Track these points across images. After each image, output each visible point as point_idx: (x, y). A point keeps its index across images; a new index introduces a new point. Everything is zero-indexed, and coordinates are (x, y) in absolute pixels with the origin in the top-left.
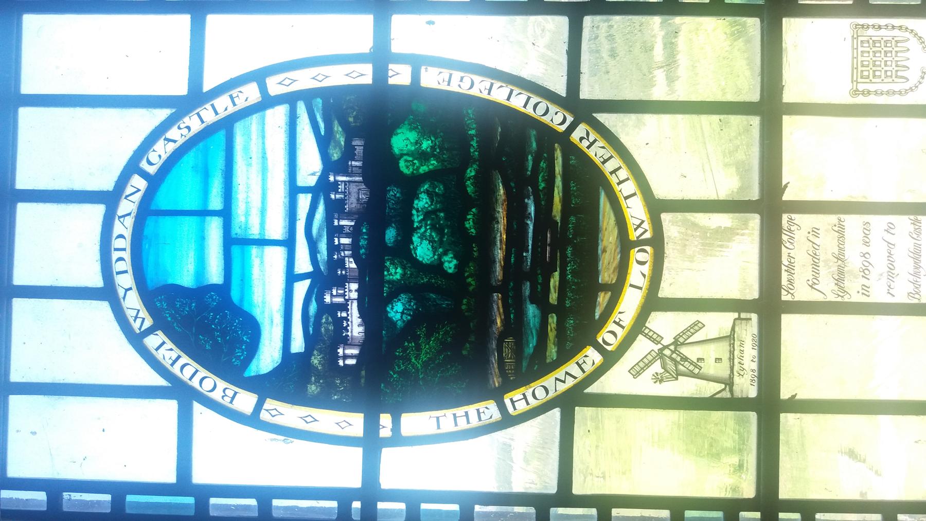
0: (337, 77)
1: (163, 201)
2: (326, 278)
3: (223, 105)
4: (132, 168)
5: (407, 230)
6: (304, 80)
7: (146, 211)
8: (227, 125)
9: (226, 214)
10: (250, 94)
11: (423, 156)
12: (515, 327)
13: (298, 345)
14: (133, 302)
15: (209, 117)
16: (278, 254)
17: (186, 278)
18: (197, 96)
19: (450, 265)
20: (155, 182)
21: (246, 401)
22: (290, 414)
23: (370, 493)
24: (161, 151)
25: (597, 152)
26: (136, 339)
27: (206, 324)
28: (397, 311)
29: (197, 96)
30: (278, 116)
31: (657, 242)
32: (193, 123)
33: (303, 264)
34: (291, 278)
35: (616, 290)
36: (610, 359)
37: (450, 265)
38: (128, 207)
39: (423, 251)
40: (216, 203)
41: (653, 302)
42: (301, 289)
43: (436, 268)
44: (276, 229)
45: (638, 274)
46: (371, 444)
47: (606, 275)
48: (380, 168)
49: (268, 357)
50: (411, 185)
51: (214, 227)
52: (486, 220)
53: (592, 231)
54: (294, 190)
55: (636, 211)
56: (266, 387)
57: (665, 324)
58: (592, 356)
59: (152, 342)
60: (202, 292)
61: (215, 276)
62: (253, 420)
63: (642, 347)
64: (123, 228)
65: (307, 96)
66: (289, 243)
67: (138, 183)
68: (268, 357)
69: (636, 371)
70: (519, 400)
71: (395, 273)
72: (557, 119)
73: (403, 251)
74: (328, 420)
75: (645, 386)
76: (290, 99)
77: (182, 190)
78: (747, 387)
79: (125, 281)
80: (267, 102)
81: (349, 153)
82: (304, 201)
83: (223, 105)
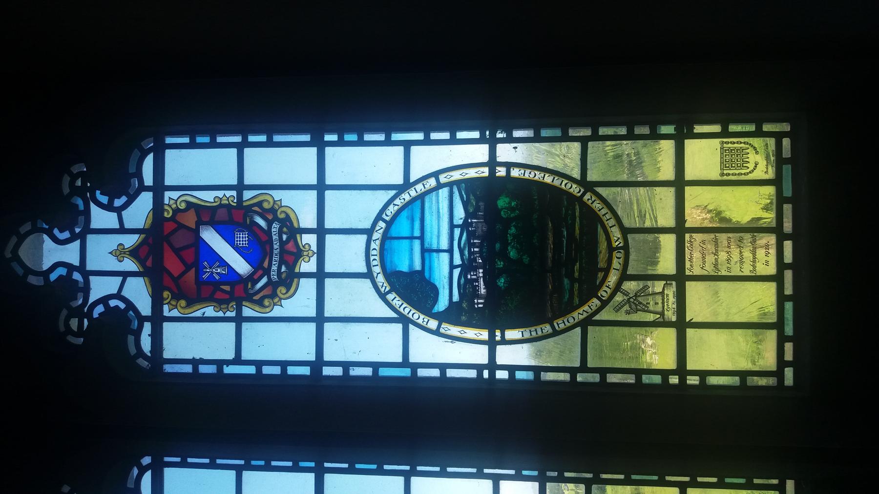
0: (472, 173)
1: (394, 232)
2: (467, 267)
3: (420, 187)
4: (379, 218)
5: (505, 244)
6: (456, 175)
7: (386, 237)
8: (421, 197)
9: (422, 238)
10: (432, 182)
11: (513, 209)
13: (456, 298)
14: (381, 279)
15: (413, 193)
16: (445, 257)
18: (407, 185)
20: (389, 224)
21: (433, 324)
22: (454, 330)
23: (492, 366)
24: (392, 209)
25: (597, 205)
26: (383, 296)
27: (414, 289)
28: (501, 282)
29: (407, 185)
30: (444, 193)
32: (406, 197)
33: (457, 261)
34: (452, 267)
35: (607, 271)
36: (604, 304)
38: (377, 235)
39: (513, 254)
40: (417, 233)
42: (457, 272)
44: (444, 245)
45: (616, 264)
46: (492, 344)
47: (602, 264)
48: (492, 215)
49: (442, 304)
50: (507, 223)
51: (417, 244)
53: (595, 243)
54: (452, 227)
56: (442, 317)
58: (595, 303)
59: (390, 297)
60: (412, 274)
61: (418, 266)
62: (437, 332)
64: (375, 246)
65: (458, 183)
66: (450, 251)
67: (382, 224)
68: (442, 304)
70: (560, 324)
72: (575, 189)
76: (450, 185)
77: (402, 227)
79: (377, 270)
80: (440, 186)
81: (477, 208)
82: (457, 232)
83: (420, 187)
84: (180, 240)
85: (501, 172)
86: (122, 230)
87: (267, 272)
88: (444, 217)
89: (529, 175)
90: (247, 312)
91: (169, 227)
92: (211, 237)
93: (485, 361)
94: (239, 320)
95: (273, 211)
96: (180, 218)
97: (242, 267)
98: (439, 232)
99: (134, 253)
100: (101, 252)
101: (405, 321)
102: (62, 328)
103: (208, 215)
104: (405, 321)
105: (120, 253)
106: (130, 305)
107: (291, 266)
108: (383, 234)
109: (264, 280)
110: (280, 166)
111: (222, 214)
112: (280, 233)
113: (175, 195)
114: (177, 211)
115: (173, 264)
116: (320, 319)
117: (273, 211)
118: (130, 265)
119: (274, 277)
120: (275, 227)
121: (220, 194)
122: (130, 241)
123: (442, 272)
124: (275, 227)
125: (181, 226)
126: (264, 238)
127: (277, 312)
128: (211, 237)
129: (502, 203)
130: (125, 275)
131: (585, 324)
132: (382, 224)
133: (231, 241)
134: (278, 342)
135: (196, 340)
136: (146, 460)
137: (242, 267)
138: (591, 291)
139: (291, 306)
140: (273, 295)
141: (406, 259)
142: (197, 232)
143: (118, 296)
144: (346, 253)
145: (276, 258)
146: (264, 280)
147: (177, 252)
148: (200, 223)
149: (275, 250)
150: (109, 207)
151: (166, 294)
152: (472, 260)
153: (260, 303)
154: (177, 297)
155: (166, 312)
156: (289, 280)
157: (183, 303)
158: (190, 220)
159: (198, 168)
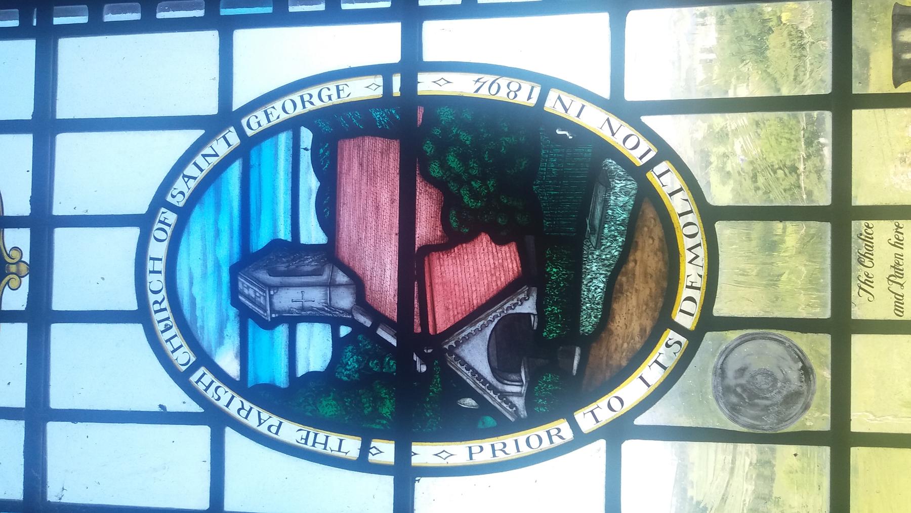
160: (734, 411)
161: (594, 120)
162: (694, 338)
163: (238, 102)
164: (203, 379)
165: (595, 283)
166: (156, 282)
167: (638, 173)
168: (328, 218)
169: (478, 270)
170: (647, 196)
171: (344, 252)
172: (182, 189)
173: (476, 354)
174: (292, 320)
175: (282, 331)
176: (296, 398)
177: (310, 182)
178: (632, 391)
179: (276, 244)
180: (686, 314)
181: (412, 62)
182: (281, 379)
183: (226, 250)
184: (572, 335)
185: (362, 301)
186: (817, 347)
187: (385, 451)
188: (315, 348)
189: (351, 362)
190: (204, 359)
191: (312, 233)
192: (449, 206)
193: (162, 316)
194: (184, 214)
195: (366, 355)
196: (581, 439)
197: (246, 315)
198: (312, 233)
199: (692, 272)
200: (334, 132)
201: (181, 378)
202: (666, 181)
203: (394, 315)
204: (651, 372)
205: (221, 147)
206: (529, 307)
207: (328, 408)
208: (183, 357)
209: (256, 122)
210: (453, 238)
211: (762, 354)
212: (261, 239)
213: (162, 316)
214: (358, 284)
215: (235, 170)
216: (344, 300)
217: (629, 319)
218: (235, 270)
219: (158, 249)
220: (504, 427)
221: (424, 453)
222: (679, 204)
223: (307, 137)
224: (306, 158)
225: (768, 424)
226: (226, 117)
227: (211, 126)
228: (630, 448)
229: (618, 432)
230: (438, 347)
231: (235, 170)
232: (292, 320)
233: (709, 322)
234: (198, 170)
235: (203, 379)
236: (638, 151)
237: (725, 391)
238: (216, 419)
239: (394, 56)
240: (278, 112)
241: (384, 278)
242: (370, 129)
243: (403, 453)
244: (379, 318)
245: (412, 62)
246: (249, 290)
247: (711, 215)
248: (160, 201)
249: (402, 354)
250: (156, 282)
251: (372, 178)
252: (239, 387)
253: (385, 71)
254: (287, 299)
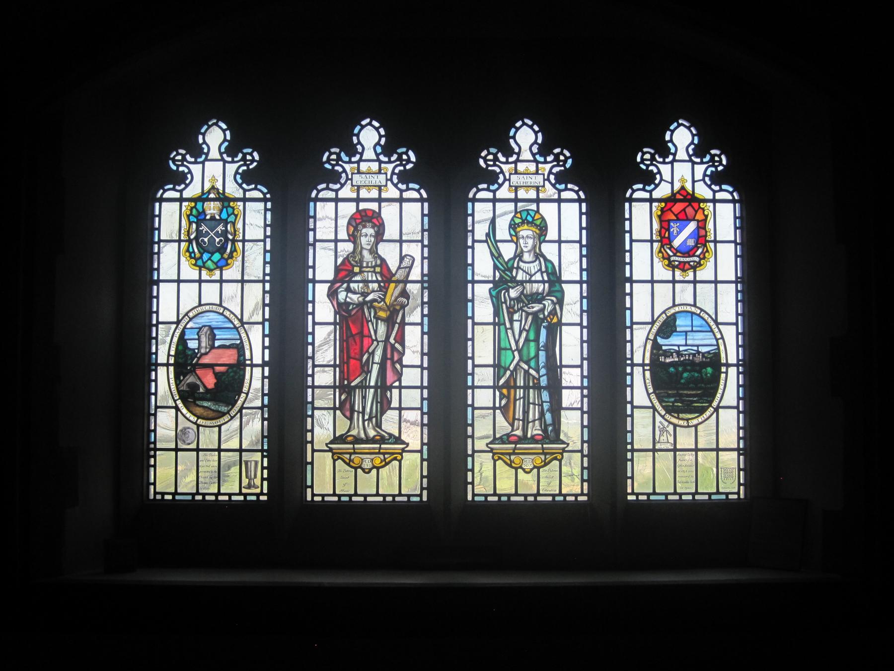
0: (723, 355)
1: (695, 317)
2: (679, 353)
3: (716, 330)
4: (702, 310)
5: (690, 371)
6: (722, 348)
7: (693, 313)
8: (712, 331)
9: (692, 331)
10: (719, 336)
11: (706, 375)
12: (669, 396)
13: (664, 348)
14: (672, 311)
15: (714, 327)
16: (683, 342)
17: (677, 323)
18: (717, 324)
19: (682, 381)
20: (699, 315)
21: (651, 337)
22: (649, 347)
23: (633, 365)
24: (706, 317)
25: (708, 413)
26: (664, 312)
27: (668, 327)
28: (672, 369)
29: (717, 324)
30: (714, 342)
31: (688, 426)
32: (712, 323)
33: (682, 348)
34: (679, 346)
35: (678, 418)
36: (663, 417)
37: (682, 381)
38: (693, 309)
39: (685, 375)
40: (694, 329)
41: (675, 426)
42: (676, 348)
43: (682, 378)
44: (689, 342)
45: (681, 423)
46: (643, 365)
47: (681, 415)
48: (703, 365)
49: (660, 341)
50: (700, 372)
51: (690, 329)
52: (693, 389)
53: (691, 412)
54: (698, 346)
55: (695, 422)
56: (655, 341)
57: (671, 428)
58: (663, 413)
59: (664, 315)
60: (675, 327)
61: (678, 329)
62: (647, 339)
63: (666, 424)
64: (688, 308)
65: (718, 349)
66: (686, 345)
67: (698, 311)
68: (660, 341)
69: (660, 422)
70: (653, 397)
71: (680, 369)
72: (715, 404)
73: (685, 370)
74: (648, 355)
75: (657, 424)
76: (718, 345)
77: (697, 322)
78: (658, 446)
79: (677, 309)
80: (717, 340)
81: (706, 358)
82: (695, 348)
83: (716, 330)
84: (690, 211)
85: (723, 369)
86: (694, 182)
87: (675, 255)
88: (703, 342)
89: (722, 382)
90: (656, 245)
91: (695, 205)
92: (692, 226)
93: (635, 362)
94: (652, 241)
95: (704, 258)
96: (700, 211)
97: (677, 243)
98: (696, 339)
99: (683, 188)
100: (683, 171)
101: (653, 323)
102: (645, 150)
103: (702, 225)
104: (653, 323)
105: (682, 180)
106: (657, 186)
107: (677, 267)
108: (694, 311)
109: (671, 254)
110: (726, 261)
111: (702, 232)
112: (694, 261)
113: (711, 209)
114: (703, 210)
115: (678, 207)
116: (652, 282)
117: (704, 258)
118: (677, 186)
119: (672, 259)
120: (697, 259)
121: (712, 232)
122: (689, 187)
123: (676, 340)
124: (697, 259)
125: (696, 212)
126: (691, 253)
127: (656, 260)
128: (692, 226)
129: (709, 370)
130: (672, 183)
131: (653, 408)
132: (698, 311)
133: (689, 237)
134: (641, 260)
135: (640, 219)
136: (581, 193)
137: (677, 243)
138: (669, 410)
139: (658, 265)
140: (664, 258)
141: (682, 323)
142: (694, 220)
143: (661, 179)
144: (685, 294)
145: (681, 259)
146: (671, 254)
147: (684, 210)
148: (698, 221)
149: (686, 260)
150: (705, 175)
151: (663, 204)
152: (682, 355)
153: (660, 251)
154: (662, 210)
155: (655, 204)
156: (671, 266)
157: (659, 213)
158: (699, 216)
159: (724, 219)
160: (181, 431)
161: (240, 403)
162: (195, 423)
163: (245, 326)
164: (186, 319)
165: (206, 404)
166: (207, 308)
167: (228, 412)
168: (220, 347)
169: (210, 381)
170: (224, 414)
171: (213, 351)
172: (227, 313)
173: (191, 379)
174: (199, 339)
175: (197, 337)
176: (182, 340)
177: (228, 343)
178: (184, 411)
179: (215, 335)
180: (200, 421)
181: (252, 366)
182: (186, 337)
183: (214, 324)
184: (196, 399)
185: (202, 355)
186: (194, 446)
187: (172, 361)
188: (193, 345)
189: (190, 353)
190: (191, 319)
191: (217, 343)
192: (223, 373)
193: (200, 309)
194: (222, 314)
195: (191, 355)
196: (175, 401)
197: (200, 329)
198: (217, 343)
199: (208, 423)
200: (240, 348)
201: (187, 314)
202: (227, 418)
203: (200, 362)
204: (188, 415)
205: (236, 322)
206: (201, 390)
207: (180, 348)
208: (191, 315)
209: (242, 331)
210: (217, 375)
211: (192, 435)
212: (216, 332)
213: (200, 309)
214: (206, 354)
215: (232, 326)
216: (203, 351)
217: (199, 411)
218: (209, 326)
219: (214, 308)
220: (177, 385)
221: (171, 369)
222: (222, 421)
223: (238, 342)
224: (233, 342)
225: (179, 436)
226: (243, 323)
227: (241, 320)
228: (174, 411)
229: (177, 409)
230: (193, 371)
231: (232, 326)
232: (199, 339)
233: (198, 426)
234: (232, 317)
235: (186, 319)
236: (232, 413)
237: (185, 429)
238: (178, 322)
239: (254, 362)
240: (244, 335)
241: (206, 360)
242: (239, 356)
243: (171, 365)
244: (199, 358)
245: (252, 366)
246: (205, 329)
247: (220, 427)
248: (225, 308)
249: (191, 364)
250: (207, 308)
251: (229, 356)
252: (185, 328)
253: (251, 360)
254: (204, 340)
